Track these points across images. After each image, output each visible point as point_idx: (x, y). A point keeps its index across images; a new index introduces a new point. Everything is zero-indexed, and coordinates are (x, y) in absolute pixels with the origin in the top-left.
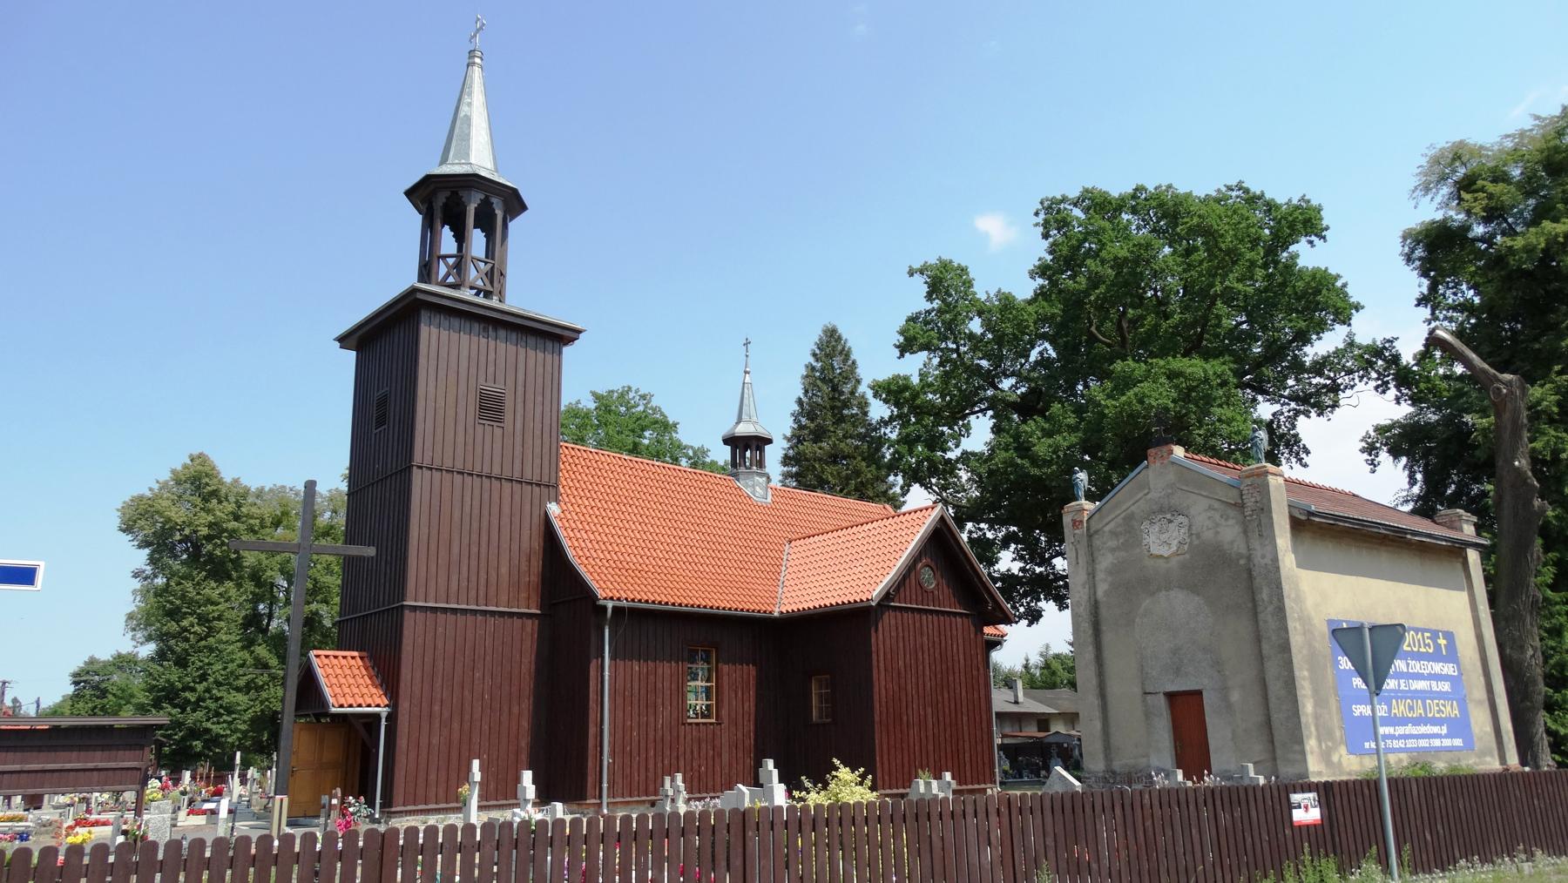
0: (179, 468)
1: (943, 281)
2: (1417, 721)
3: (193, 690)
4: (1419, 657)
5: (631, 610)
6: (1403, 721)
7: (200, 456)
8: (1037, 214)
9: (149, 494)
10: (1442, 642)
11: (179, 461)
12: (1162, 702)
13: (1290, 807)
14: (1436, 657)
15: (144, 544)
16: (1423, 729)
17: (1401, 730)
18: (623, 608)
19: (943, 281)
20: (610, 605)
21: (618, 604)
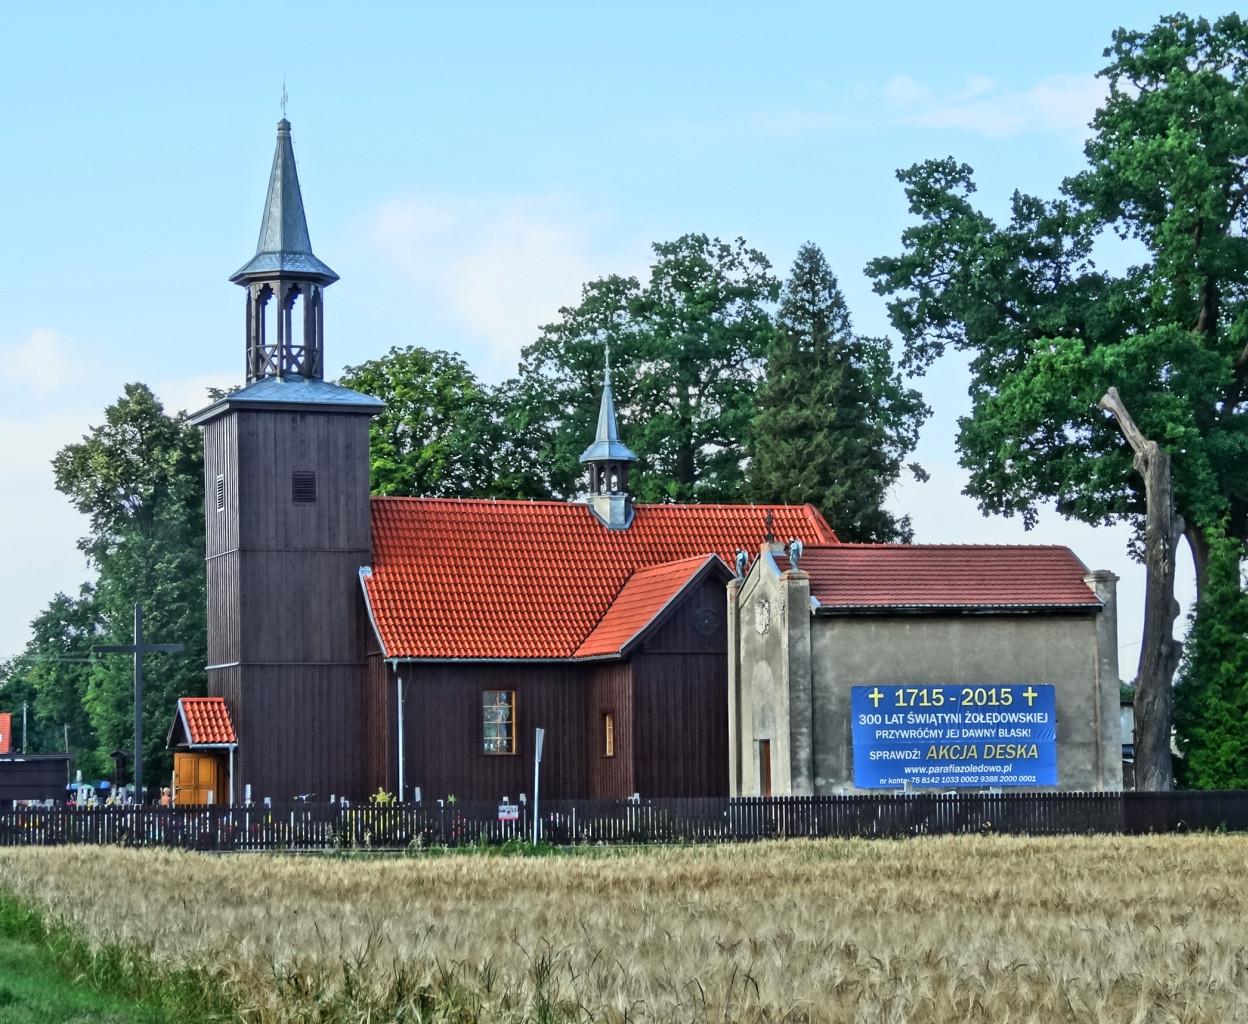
0: (116, 404)
1: (933, 188)
2: (958, 763)
3: (159, 689)
4: (986, 709)
5: (413, 664)
6: (943, 762)
7: (138, 386)
8: (1107, 53)
9: (83, 443)
10: (1030, 694)
11: (115, 395)
12: (757, 745)
13: (497, 811)
14: (1020, 705)
15: (85, 508)
16: (973, 769)
17: (932, 770)
18: (407, 664)
19: (933, 188)
20: (395, 661)
21: (403, 660)
